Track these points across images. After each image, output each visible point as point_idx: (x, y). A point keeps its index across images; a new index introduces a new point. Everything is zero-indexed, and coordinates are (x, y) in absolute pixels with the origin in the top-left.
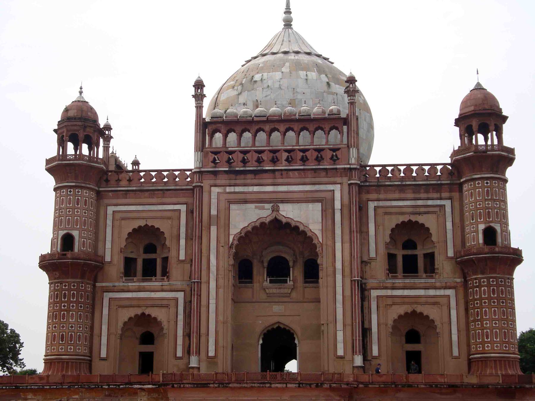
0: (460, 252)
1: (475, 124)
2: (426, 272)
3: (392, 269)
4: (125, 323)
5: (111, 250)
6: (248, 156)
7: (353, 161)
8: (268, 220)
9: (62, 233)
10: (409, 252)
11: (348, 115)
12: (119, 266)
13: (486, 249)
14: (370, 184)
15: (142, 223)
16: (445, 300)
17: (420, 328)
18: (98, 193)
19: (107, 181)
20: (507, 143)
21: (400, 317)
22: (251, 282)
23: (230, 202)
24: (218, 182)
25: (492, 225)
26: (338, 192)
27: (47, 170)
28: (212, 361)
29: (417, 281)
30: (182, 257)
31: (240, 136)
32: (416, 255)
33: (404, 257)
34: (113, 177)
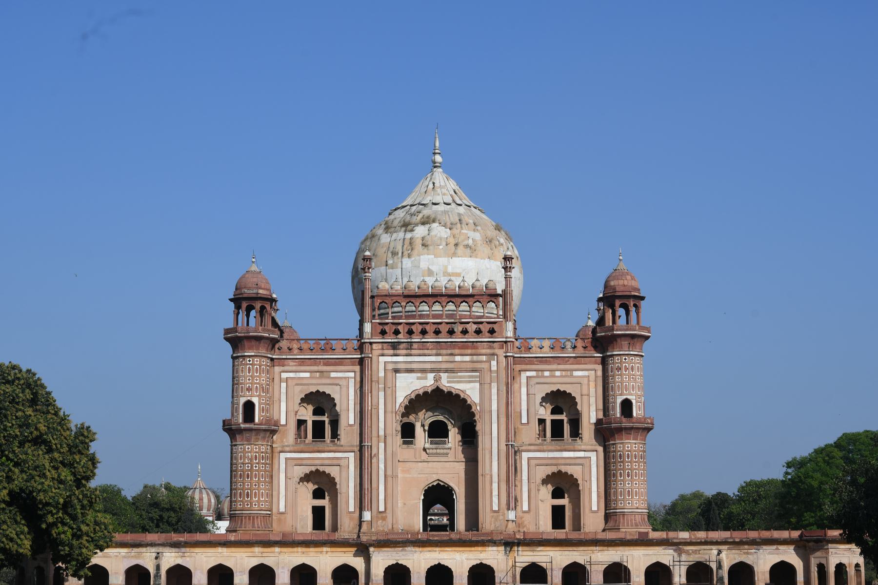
0: (601, 420)
1: (618, 303)
2: (571, 436)
9: (243, 400)
11: (504, 291)
12: (293, 426)
13: (624, 420)
15: (314, 389)
20: (642, 324)
21: (548, 476)
23: (397, 371)
25: (629, 397)
27: (226, 339)
28: (382, 515)
30: (351, 422)
33: (552, 421)
34: (284, 344)
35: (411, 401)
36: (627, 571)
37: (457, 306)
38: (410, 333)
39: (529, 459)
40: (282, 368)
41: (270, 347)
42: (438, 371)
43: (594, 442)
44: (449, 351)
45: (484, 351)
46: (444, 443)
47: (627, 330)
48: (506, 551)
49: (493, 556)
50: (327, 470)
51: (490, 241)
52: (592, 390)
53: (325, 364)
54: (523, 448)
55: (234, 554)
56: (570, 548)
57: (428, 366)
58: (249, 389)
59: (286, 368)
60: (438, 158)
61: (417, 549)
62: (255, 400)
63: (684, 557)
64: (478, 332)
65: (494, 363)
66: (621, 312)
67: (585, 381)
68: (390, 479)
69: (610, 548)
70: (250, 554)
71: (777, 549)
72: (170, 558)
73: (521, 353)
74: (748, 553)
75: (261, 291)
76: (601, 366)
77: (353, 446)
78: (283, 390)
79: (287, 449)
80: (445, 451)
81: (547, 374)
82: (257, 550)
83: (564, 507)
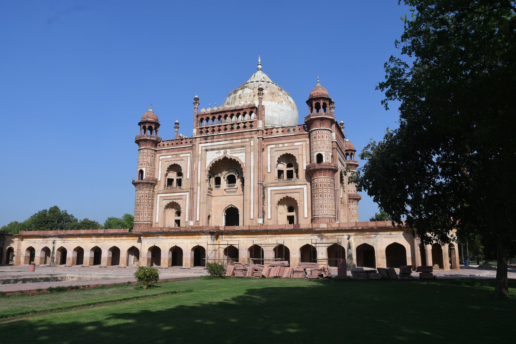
6: (215, 128)
17: (293, 206)
21: (281, 200)
23: (207, 150)
24: (202, 142)
25: (321, 152)
30: (188, 177)
34: (161, 143)
35: (213, 164)
36: (287, 251)
38: (213, 131)
39: (271, 191)
40: (160, 154)
41: (154, 145)
42: (226, 148)
43: (305, 180)
44: (231, 138)
45: (247, 136)
47: (318, 115)
48: (211, 238)
49: (204, 241)
50: (177, 201)
51: (273, 94)
52: (304, 152)
53: (178, 151)
54: (268, 185)
55: (84, 241)
56: (252, 236)
57: (221, 147)
58: (141, 164)
59: (162, 154)
60: (260, 67)
61: (164, 237)
62: (144, 169)
63: (325, 241)
64: (245, 127)
65: (252, 142)
67: (301, 147)
68: (202, 204)
69: (276, 236)
70: (91, 241)
71: (391, 234)
72: (59, 243)
73: (267, 136)
74: (369, 238)
75: (149, 119)
76: (308, 139)
77: (188, 189)
78: (160, 165)
79: (160, 192)
80: (234, 190)
81: (280, 145)
82: (94, 239)
83: (293, 216)
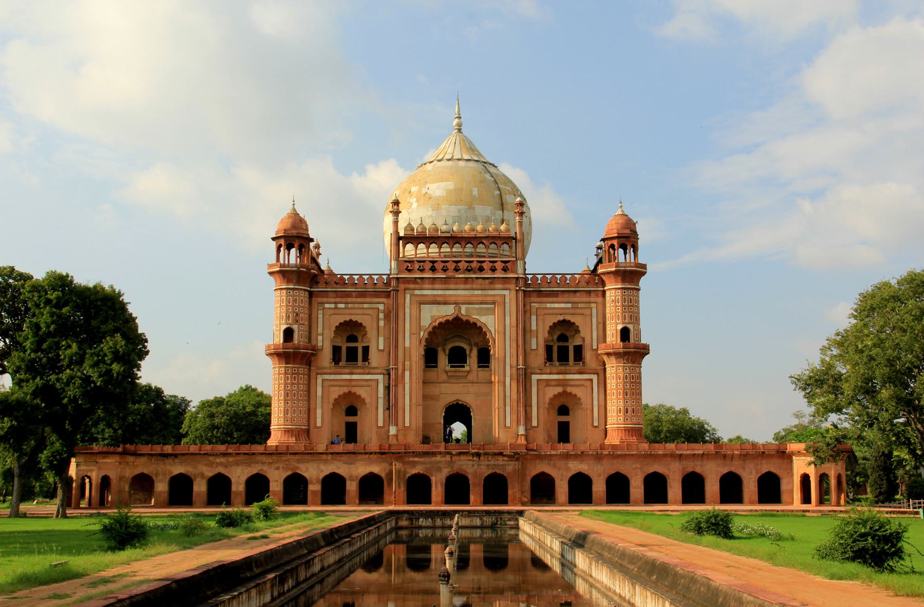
2: (575, 360)
3: (549, 358)
4: (335, 400)
5: (324, 340)
7: (520, 271)
8: (451, 318)
9: (284, 327)
10: (561, 344)
14: (534, 290)
16: (589, 383)
18: (311, 294)
19: (317, 283)
20: (641, 261)
21: (555, 396)
22: (436, 367)
23: (421, 304)
26: (509, 295)
29: (568, 368)
30: (381, 347)
31: (428, 248)
32: (567, 347)
34: (322, 281)
37: (475, 247)
46: (463, 367)
62: (295, 327)
66: (621, 251)
